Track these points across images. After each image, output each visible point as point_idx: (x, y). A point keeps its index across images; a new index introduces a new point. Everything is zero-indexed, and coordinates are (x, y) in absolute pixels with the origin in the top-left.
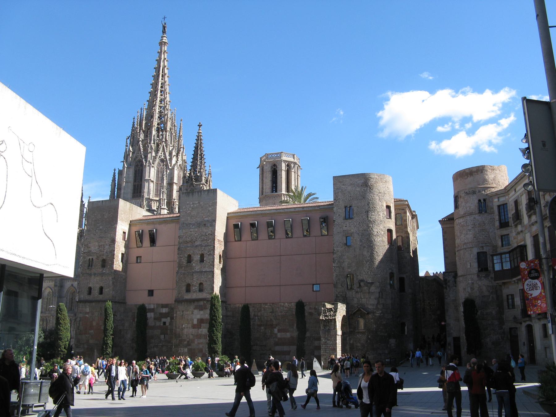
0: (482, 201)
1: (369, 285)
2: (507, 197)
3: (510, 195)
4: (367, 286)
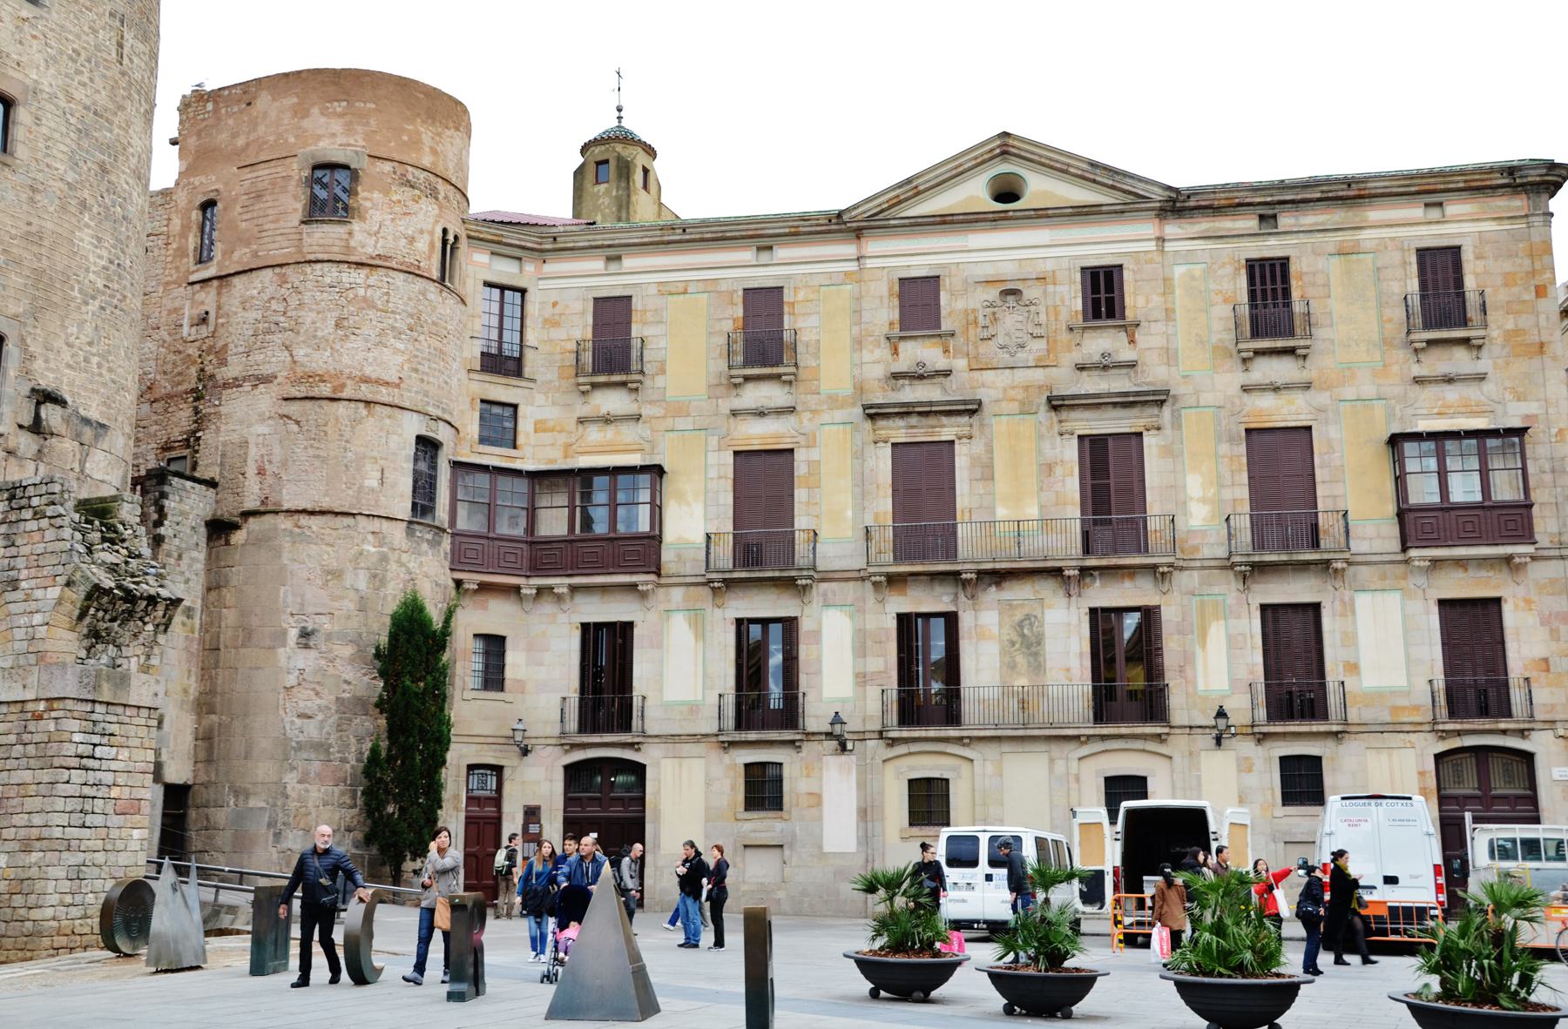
0: (451, 238)
1: (88, 433)
2: (529, 268)
3: (549, 268)
4: (77, 436)
